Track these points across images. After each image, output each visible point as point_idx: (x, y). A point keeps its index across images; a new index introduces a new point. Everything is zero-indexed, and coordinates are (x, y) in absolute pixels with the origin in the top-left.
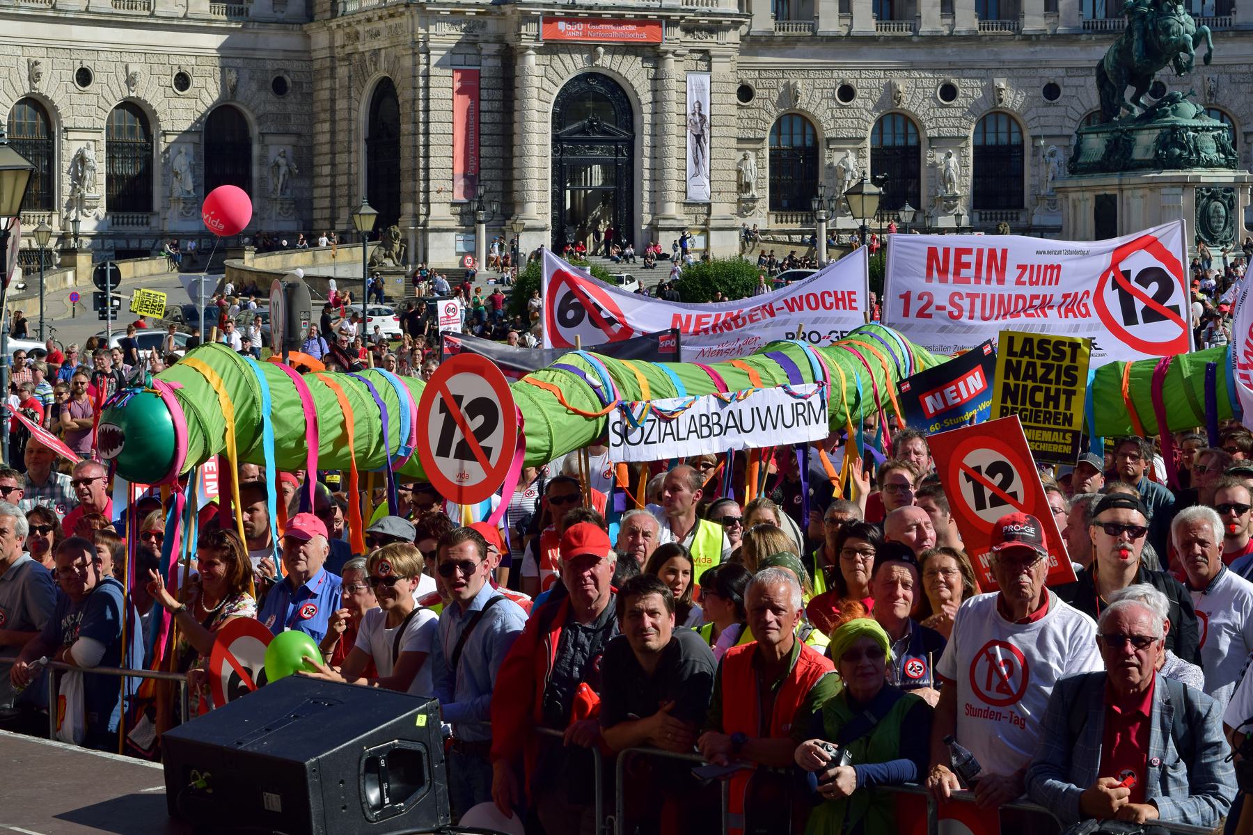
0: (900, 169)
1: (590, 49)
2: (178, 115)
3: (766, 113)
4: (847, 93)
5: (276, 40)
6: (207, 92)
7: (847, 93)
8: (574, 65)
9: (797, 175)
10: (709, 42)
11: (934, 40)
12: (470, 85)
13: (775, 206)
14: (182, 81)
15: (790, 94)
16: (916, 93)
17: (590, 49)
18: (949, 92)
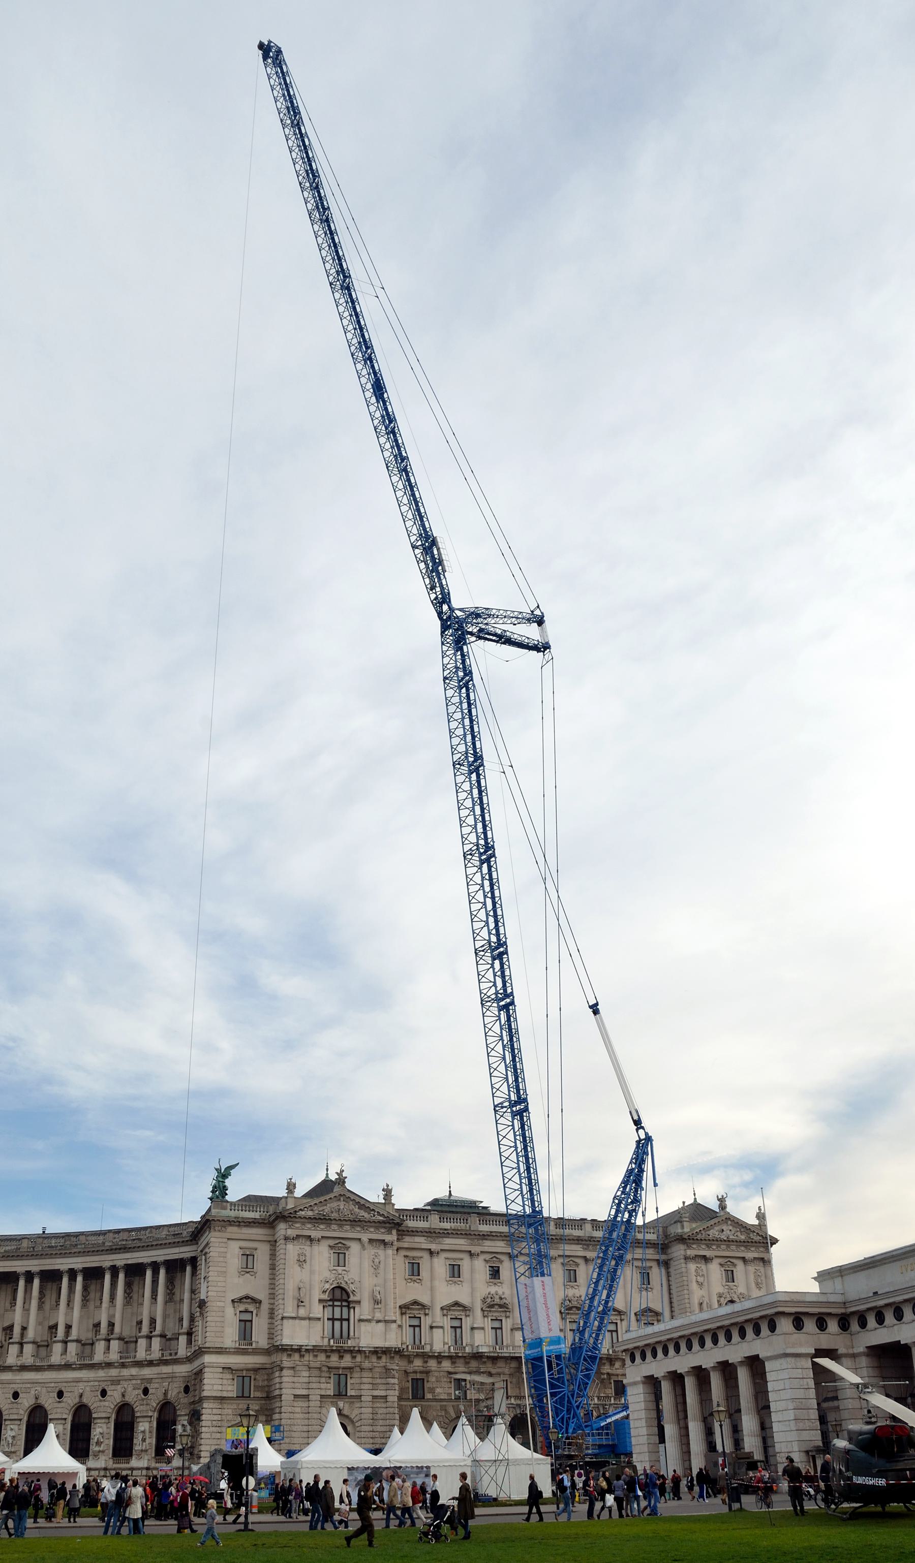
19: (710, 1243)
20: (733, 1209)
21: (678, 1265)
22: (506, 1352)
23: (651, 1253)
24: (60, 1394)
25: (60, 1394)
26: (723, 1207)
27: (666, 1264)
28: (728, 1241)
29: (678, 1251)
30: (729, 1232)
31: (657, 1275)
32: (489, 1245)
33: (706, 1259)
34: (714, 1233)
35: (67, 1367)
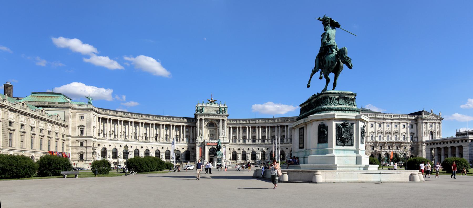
0: (244, 156)
1: (212, 145)
2: (182, 151)
3: (232, 151)
4: (249, 149)
5: (193, 145)
6: (186, 149)
7: (249, 149)
8: (211, 147)
9: (234, 157)
10: (226, 145)
11: (257, 144)
12: (201, 148)
13: (242, 159)
14: (183, 148)
15: (243, 149)
16: (255, 149)
17: (212, 145)
18: (258, 149)
19: (428, 120)
20: (434, 112)
21: (419, 124)
22: (382, 141)
23: (414, 122)
24: (287, 149)
25: (287, 149)
26: (432, 112)
27: (417, 124)
28: (432, 120)
29: (420, 121)
30: (433, 117)
31: (415, 126)
32: (379, 120)
33: (426, 123)
34: (429, 118)
35: (288, 143)
